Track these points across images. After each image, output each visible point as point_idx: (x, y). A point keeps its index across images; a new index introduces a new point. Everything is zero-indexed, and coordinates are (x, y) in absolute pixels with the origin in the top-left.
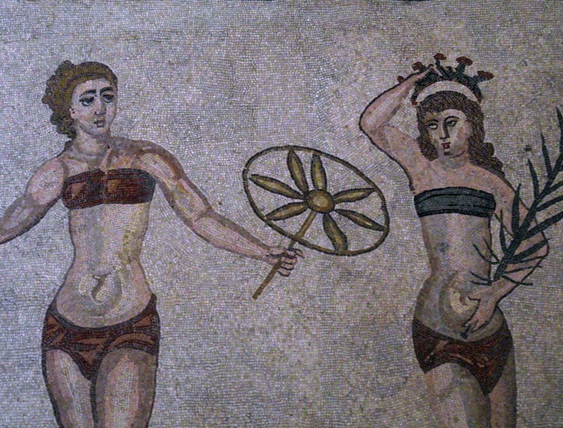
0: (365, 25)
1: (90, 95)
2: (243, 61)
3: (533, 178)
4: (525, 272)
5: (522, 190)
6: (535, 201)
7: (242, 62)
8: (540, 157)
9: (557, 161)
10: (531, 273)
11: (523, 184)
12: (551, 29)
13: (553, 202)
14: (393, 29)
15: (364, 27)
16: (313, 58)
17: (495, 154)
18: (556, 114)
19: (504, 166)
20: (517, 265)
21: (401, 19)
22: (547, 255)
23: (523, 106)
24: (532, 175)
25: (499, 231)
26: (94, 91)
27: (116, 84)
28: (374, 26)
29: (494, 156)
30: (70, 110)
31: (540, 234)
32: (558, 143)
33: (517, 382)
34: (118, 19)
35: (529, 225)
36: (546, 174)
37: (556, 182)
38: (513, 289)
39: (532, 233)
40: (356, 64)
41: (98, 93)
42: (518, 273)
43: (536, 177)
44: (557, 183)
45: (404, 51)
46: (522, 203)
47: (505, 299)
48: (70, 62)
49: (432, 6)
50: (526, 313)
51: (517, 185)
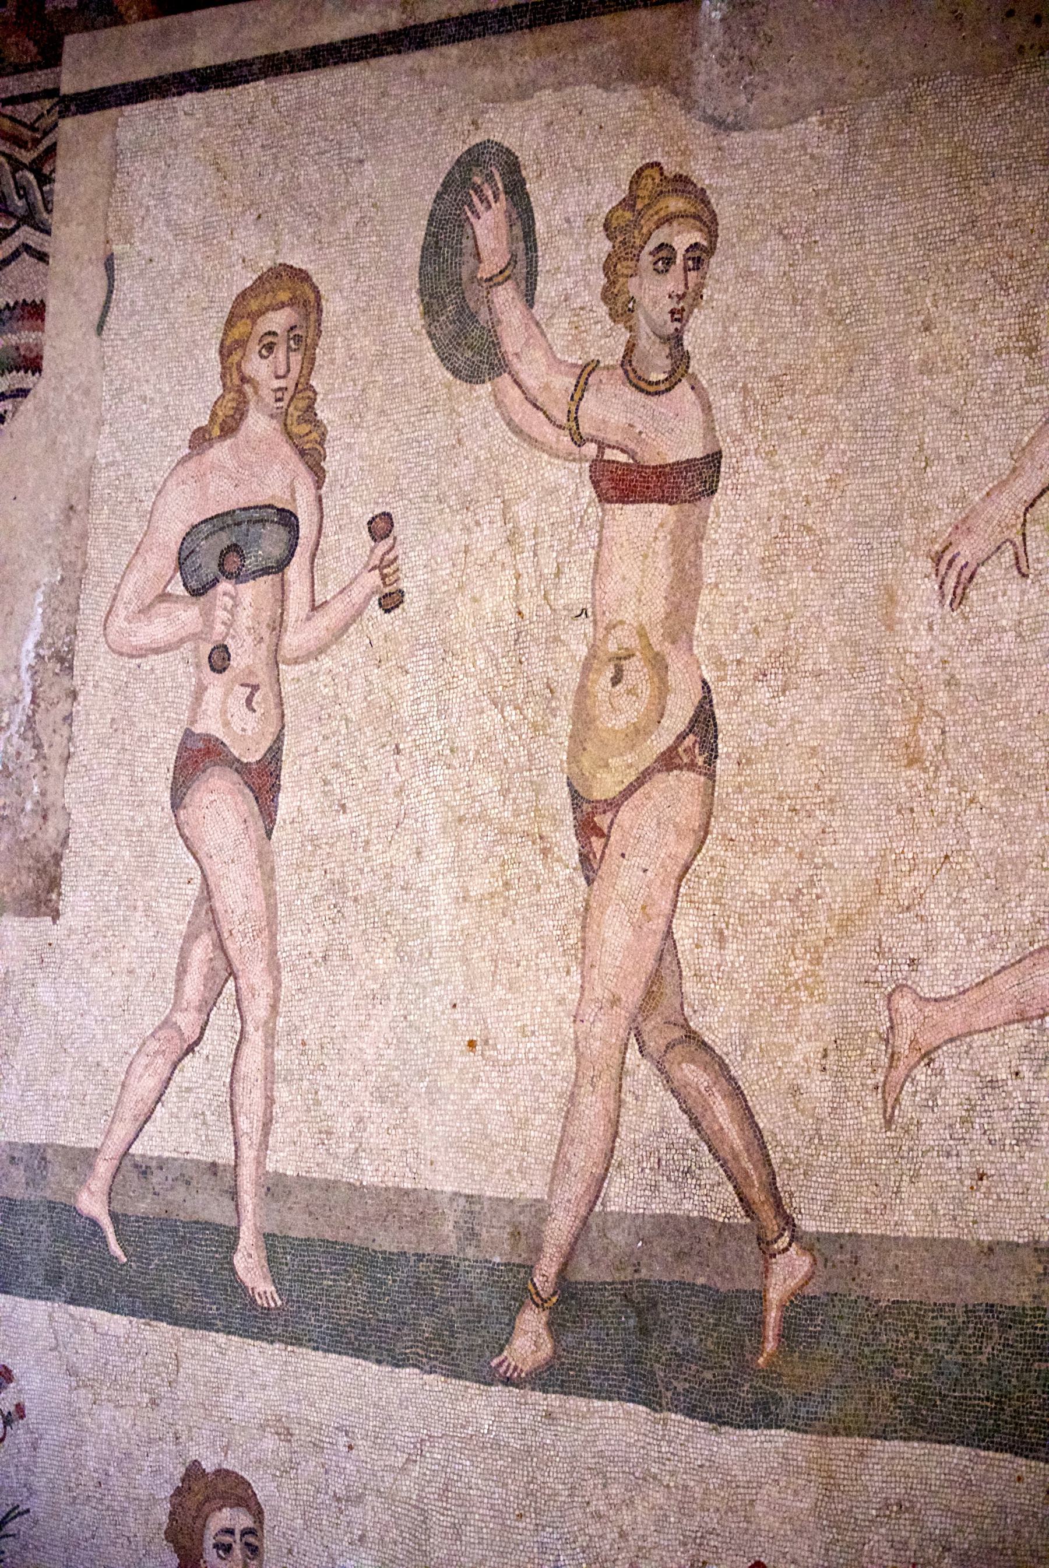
0: (639, 1470)
1: (227, 1539)
2: (443, 1515)
7: (442, 1518)
12: (971, 1538)
14: (686, 1487)
15: (637, 1474)
16: (551, 1530)
21: (701, 1466)
26: (230, 1532)
27: (261, 1523)
28: (655, 1478)
30: (202, 1561)
34: (264, 1387)
40: (617, 1559)
41: (238, 1537)
45: (700, 1545)
48: (199, 1463)
49: (758, 1444)
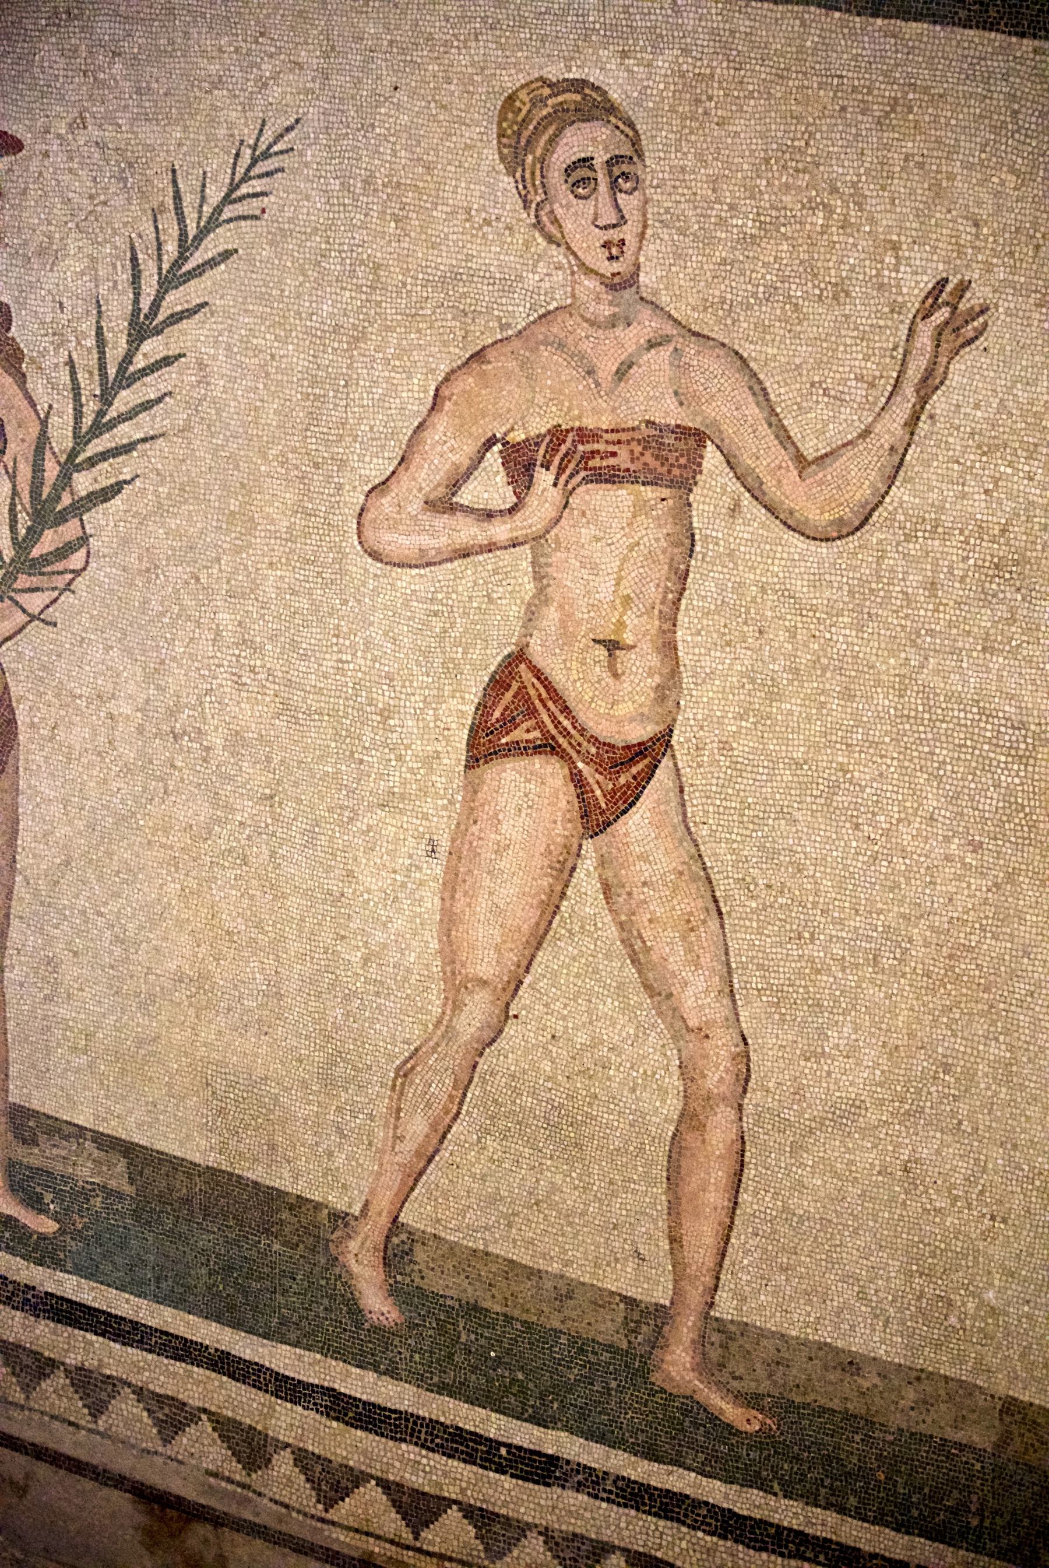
3: (75, 395)
4: (46, 597)
5: (54, 420)
6: (74, 448)
8: (89, 350)
9: (120, 364)
10: (55, 600)
11: (55, 406)
13: (104, 456)
17: (13, 329)
18: (129, 255)
19: (27, 359)
20: (34, 579)
22: (84, 569)
23: (70, 225)
24: (73, 389)
25: (9, 500)
29: (10, 335)
31: (76, 521)
32: (126, 324)
33: (20, 810)
35: (60, 498)
36: (98, 392)
37: (112, 413)
38: (23, 627)
39: (62, 518)
42: (35, 595)
43: (80, 394)
44: (115, 414)
46: (51, 448)
47: (9, 643)
50: (41, 680)
51: (46, 405)
